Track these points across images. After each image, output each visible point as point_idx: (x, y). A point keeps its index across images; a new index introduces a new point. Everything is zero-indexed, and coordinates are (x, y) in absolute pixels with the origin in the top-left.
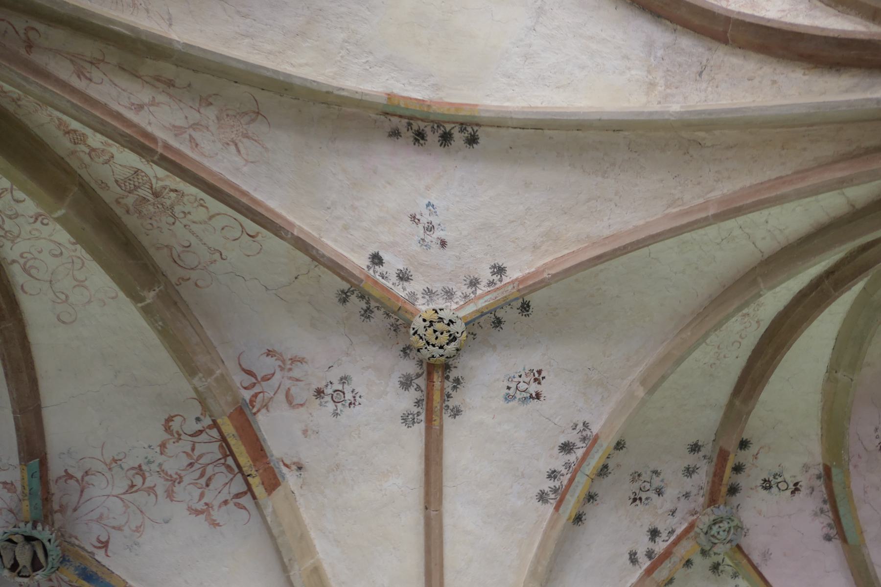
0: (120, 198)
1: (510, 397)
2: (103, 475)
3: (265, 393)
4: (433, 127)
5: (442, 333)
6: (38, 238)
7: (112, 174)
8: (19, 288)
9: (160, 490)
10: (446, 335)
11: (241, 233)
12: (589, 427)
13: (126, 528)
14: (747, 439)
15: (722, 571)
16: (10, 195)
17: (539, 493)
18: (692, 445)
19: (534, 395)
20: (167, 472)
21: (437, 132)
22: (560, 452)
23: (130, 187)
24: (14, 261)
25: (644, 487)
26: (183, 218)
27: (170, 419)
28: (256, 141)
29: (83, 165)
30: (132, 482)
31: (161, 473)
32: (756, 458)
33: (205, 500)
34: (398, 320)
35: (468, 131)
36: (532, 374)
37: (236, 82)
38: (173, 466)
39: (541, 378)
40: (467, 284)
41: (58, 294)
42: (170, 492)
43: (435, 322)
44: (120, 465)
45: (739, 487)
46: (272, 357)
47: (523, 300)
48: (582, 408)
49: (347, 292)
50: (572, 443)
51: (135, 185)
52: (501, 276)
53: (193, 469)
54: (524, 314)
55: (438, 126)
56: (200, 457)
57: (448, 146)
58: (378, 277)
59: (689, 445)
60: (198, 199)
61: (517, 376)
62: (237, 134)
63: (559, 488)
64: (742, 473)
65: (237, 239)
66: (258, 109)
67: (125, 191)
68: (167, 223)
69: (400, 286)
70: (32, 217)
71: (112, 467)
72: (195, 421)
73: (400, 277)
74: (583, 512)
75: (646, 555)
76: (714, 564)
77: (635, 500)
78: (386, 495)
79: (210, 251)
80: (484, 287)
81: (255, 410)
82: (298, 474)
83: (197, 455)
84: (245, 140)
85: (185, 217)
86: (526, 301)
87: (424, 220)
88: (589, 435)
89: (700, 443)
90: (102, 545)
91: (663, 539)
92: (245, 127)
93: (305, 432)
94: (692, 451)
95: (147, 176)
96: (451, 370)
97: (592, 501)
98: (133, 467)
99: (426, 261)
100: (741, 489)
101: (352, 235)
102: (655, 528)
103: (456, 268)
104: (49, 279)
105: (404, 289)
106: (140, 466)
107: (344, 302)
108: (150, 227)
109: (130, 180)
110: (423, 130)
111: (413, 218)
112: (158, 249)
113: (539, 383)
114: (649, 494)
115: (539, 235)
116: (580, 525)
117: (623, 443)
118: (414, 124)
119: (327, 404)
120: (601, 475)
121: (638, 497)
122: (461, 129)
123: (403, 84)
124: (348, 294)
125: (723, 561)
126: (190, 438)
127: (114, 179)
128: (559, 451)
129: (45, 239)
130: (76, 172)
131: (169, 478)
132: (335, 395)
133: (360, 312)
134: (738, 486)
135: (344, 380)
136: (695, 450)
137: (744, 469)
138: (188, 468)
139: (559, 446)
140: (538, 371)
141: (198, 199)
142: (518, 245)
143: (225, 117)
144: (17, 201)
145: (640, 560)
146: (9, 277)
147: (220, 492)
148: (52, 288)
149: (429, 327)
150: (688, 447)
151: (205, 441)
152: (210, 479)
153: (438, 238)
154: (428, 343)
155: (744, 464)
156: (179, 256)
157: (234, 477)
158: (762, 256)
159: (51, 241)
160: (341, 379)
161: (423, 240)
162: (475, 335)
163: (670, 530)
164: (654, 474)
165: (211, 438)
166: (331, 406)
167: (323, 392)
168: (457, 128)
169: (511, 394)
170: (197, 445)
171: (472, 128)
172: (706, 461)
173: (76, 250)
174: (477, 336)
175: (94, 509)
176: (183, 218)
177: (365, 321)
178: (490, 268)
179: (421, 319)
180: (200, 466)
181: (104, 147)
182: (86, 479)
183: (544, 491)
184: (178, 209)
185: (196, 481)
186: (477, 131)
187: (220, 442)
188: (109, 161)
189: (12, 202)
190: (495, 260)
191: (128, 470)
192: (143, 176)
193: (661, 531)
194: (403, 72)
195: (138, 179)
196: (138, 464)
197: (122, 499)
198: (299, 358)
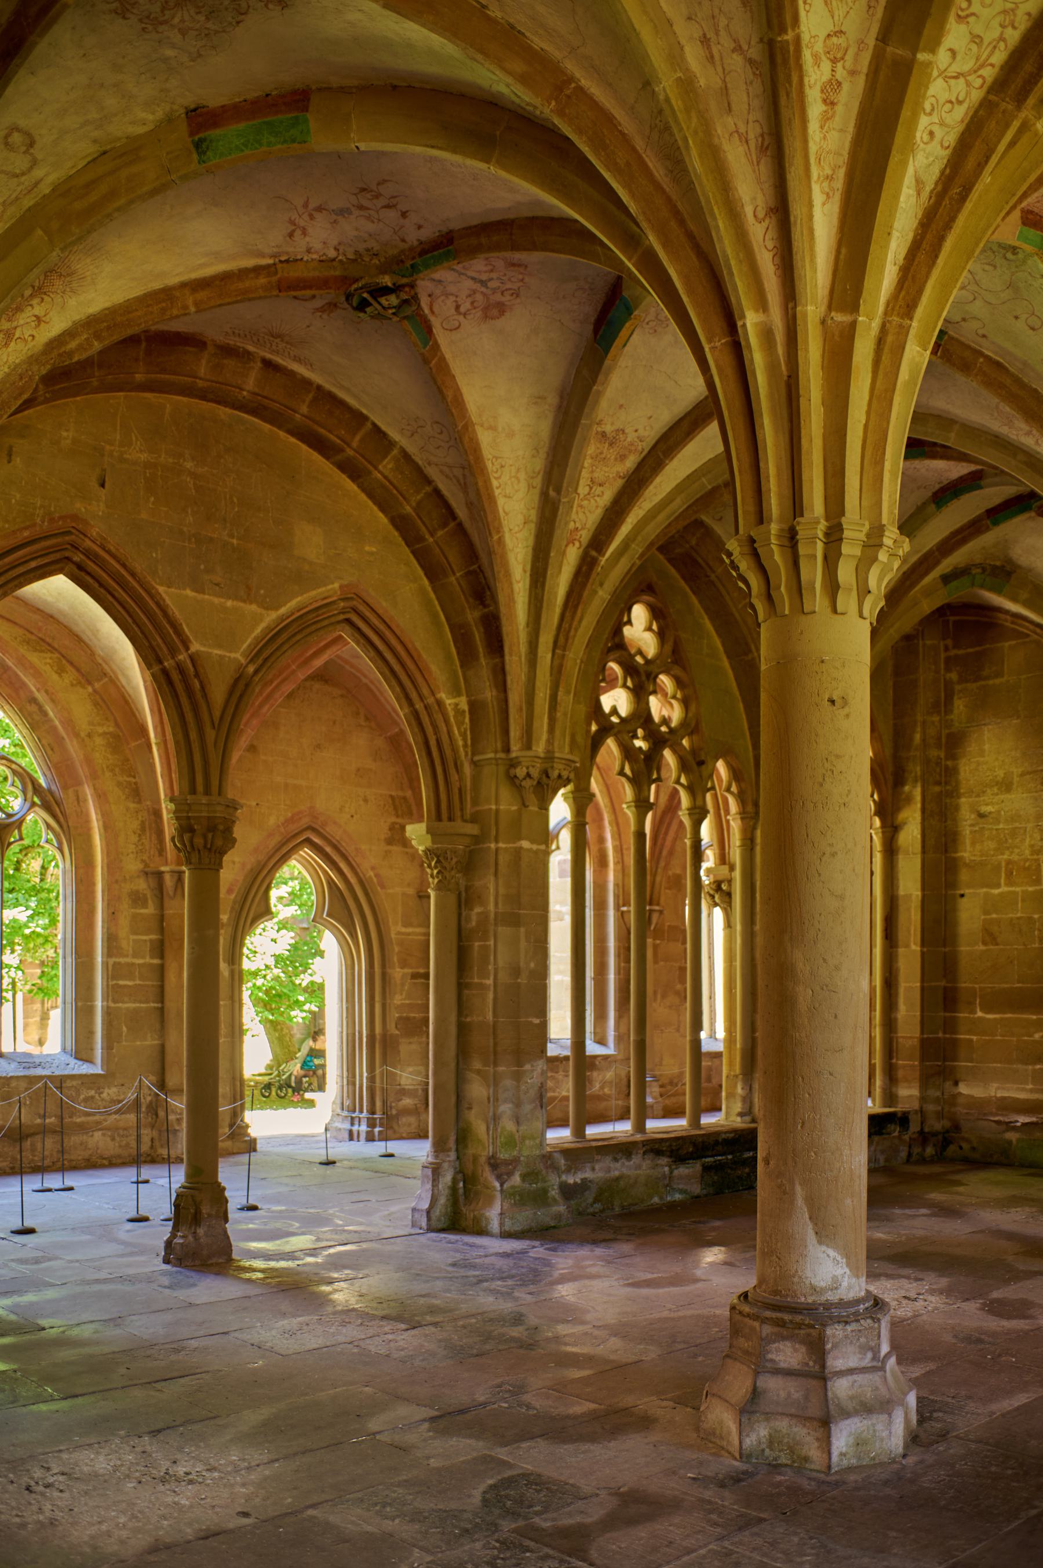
16: (950, 69)
181: (824, 58)
188: (835, 33)
189: (959, 58)
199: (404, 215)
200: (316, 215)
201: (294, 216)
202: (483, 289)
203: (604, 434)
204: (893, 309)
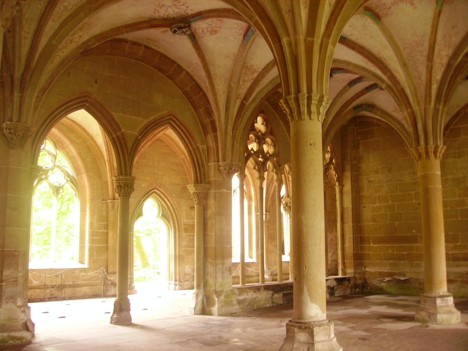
199: (187, 7)
200: (162, 7)
201: (156, 8)
202: (211, 27)
203: (247, 67)
204: (324, 36)
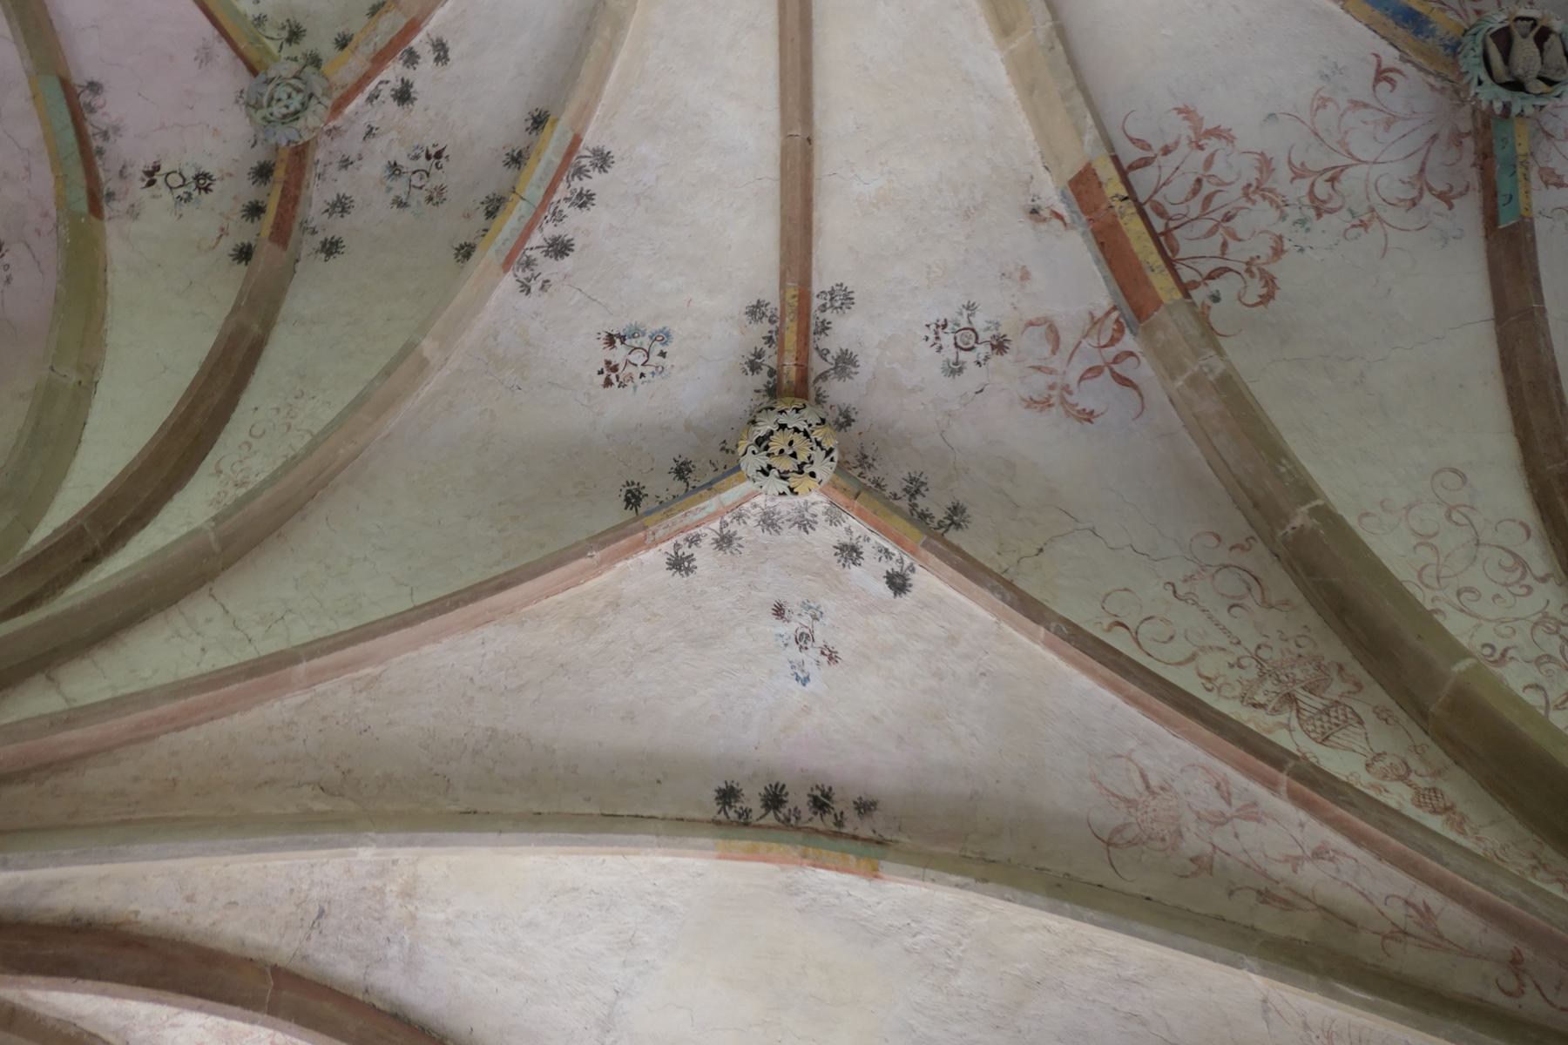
0: (1354, 693)
1: (661, 338)
2: (1384, 200)
3: (1096, 345)
4: (797, 819)
5: (782, 451)
6: (1501, 621)
7: (1369, 735)
8: (1535, 532)
9: (1283, 172)
10: (774, 448)
11: (1139, 631)
12: (520, 284)
13: (1344, 105)
14: (239, 262)
15: (284, 28)
17: (609, 167)
18: (336, 252)
19: (618, 342)
20: (1271, 205)
21: (790, 810)
22: (572, 239)
23: (1336, 711)
24: (1544, 580)
25: (421, 179)
26: (1242, 657)
27: (1266, 299)
28: (1113, 795)
29: (1421, 752)
30: (1333, 187)
31: (1281, 203)
32: (222, 230)
33: (1202, 156)
34: (860, 475)
35: (736, 811)
36: (621, 380)
37: (1148, 899)
38: (1261, 215)
39: (606, 372)
40: (736, 539)
41: (1466, 522)
42: (1265, 169)
43: (794, 471)
44: (1354, 217)
45: (253, 177)
46: (1084, 410)
47: (636, 510)
48: (532, 318)
49: (950, 525)
50: (551, 257)
51: (1328, 715)
52: (676, 553)
53: (1224, 211)
54: (635, 487)
55: (789, 820)
56: (1212, 232)
57: (771, 786)
58: (896, 552)
59: (343, 253)
60: (1215, 691)
61: (648, 376)
62: (1147, 806)
63: (573, 176)
64: (247, 204)
65: (1146, 619)
66: (1109, 851)
67: (1346, 706)
68: (1271, 648)
69: (856, 535)
70: (1512, 658)
71: (1369, 215)
72: (1222, 296)
73: (856, 551)
74: (530, 133)
75: (418, 57)
76: (298, 41)
77: (438, 155)
78: (881, 164)
79: (1195, 598)
80: (706, 535)
81: (1115, 315)
82: (1038, 202)
83: (1217, 234)
84: (1132, 795)
85: (1239, 659)
86: (631, 509)
87: (813, 653)
88: (520, 270)
89: (323, 256)
90: (1386, 74)
91: (389, 85)
92: (1133, 820)
93: (1025, 276)
94: (337, 242)
95: (1307, 733)
96: (765, 386)
97: (515, 154)
98: (1330, 213)
99: (809, 580)
100: (249, 174)
101: (942, 627)
102: (403, 105)
103: (757, 567)
104: (1481, 549)
105: (849, 530)
106: (1319, 215)
107: (955, 508)
108: (1302, 641)
109: (1337, 725)
110: (816, 813)
111: (832, 657)
112: (1287, 603)
113: (608, 363)
114: (413, 165)
115: (609, 626)
116: (537, 110)
117: (460, 257)
118: (832, 825)
119: (986, 325)
120: (499, 200)
121: (432, 160)
122: (747, 816)
123: (850, 895)
124: (948, 522)
125: (281, 47)
126: (1230, 265)
127: (1366, 726)
128: (572, 242)
129: (1489, 620)
130: (1432, 739)
131: (1267, 193)
132: (972, 343)
133: (927, 490)
134: (254, 179)
135: (956, 369)
136: (332, 243)
137: (245, 211)
138: (1234, 212)
139: (573, 250)
140: (612, 384)
141: (1215, 691)
142: (646, 609)
143: (1167, 838)
144: (1537, 687)
145: (429, 47)
146: (1552, 552)
147: (1177, 168)
148: (1476, 533)
149: (804, 463)
150: (343, 250)
151: (1202, 260)
152: (1195, 192)
153: (788, 621)
154: (806, 434)
155: (244, 219)
156: (1250, 590)
157: (1151, 197)
158: (211, 589)
159: (1477, 617)
160: (960, 370)
161: (815, 618)
162: (722, 449)
163: (375, 102)
164: (404, 201)
165: (1192, 265)
166: (979, 322)
167: (993, 347)
168: (754, 818)
169: (658, 343)
170: (1218, 253)
171: (728, 818)
172: (312, 225)
173: (1433, 601)
174: (720, 448)
175: (1400, 138)
176: (1242, 657)
177: (919, 473)
178: (696, 568)
179: (818, 477)
180: (1213, 215)
181: (1385, 783)
182: (1415, 193)
183: (600, 171)
184: (1252, 673)
185: (1219, 188)
186: (719, 813)
187: (1177, 257)
188: (1374, 759)
189: (1546, 685)
190: (687, 582)
191: (1341, 208)
192: (1314, 731)
193: (391, 99)
194: (850, 917)
195: (1322, 727)
196: (1322, 219)
197: (1353, 157)
198: (1036, 408)
